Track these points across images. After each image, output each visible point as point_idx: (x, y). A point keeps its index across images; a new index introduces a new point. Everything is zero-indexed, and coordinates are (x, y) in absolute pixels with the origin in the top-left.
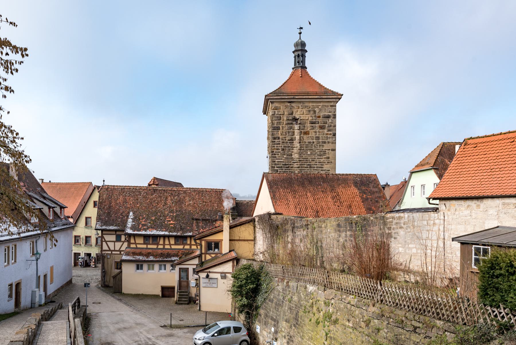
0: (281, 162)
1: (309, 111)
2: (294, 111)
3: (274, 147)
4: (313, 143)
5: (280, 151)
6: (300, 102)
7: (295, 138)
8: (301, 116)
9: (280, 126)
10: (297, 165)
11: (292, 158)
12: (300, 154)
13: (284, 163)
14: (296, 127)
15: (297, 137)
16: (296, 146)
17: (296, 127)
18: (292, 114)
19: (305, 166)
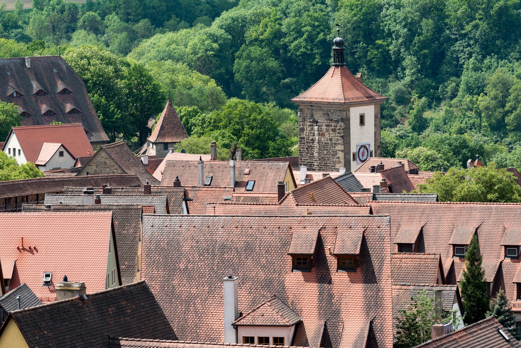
0: (306, 160)
1: (324, 114)
2: (315, 113)
3: (301, 145)
4: (328, 143)
5: (305, 149)
6: (318, 106)
7: (315, 138)
8: (319, 118)
9: (305, 127)
10: (317, 163)
11: (314, 156)
12: (319, 153)
13: (308, 161)
14: (316, 128)
15: (317, 138)
16: (316, 146)
17: (316, 128)
18: (313, 116)
19: (323, 164)
